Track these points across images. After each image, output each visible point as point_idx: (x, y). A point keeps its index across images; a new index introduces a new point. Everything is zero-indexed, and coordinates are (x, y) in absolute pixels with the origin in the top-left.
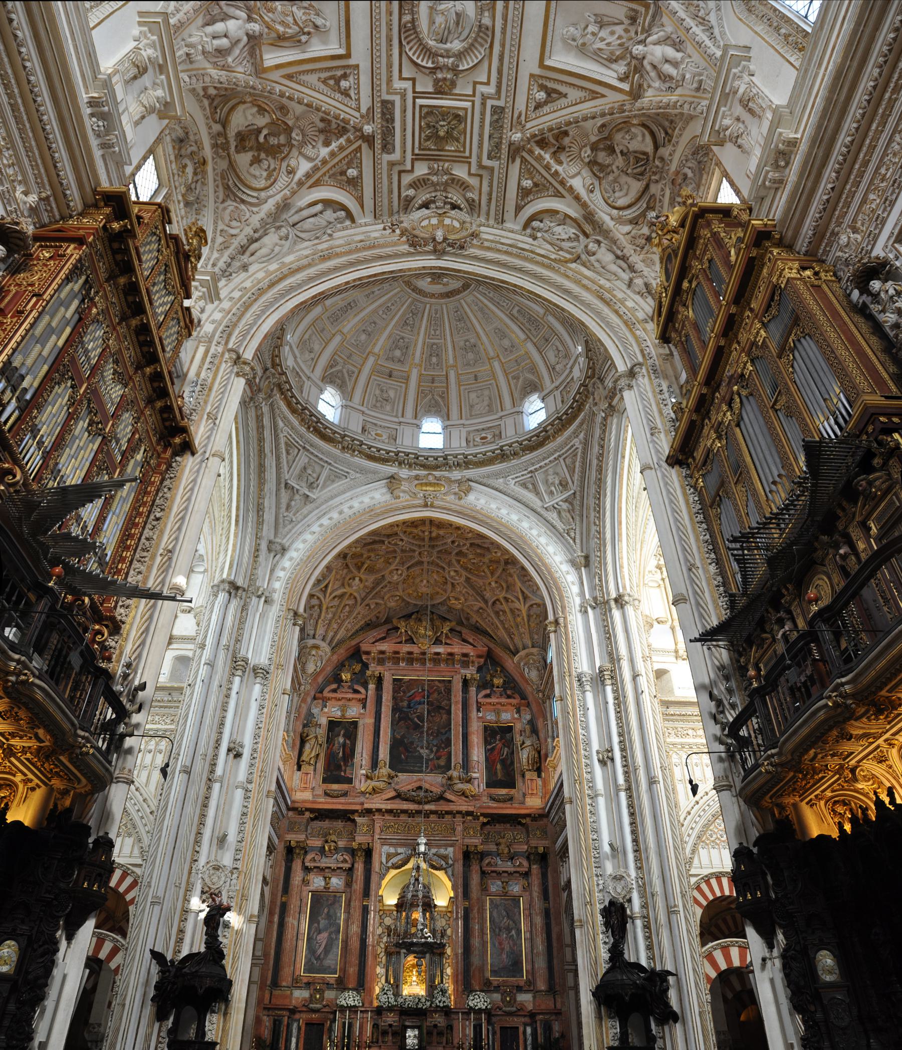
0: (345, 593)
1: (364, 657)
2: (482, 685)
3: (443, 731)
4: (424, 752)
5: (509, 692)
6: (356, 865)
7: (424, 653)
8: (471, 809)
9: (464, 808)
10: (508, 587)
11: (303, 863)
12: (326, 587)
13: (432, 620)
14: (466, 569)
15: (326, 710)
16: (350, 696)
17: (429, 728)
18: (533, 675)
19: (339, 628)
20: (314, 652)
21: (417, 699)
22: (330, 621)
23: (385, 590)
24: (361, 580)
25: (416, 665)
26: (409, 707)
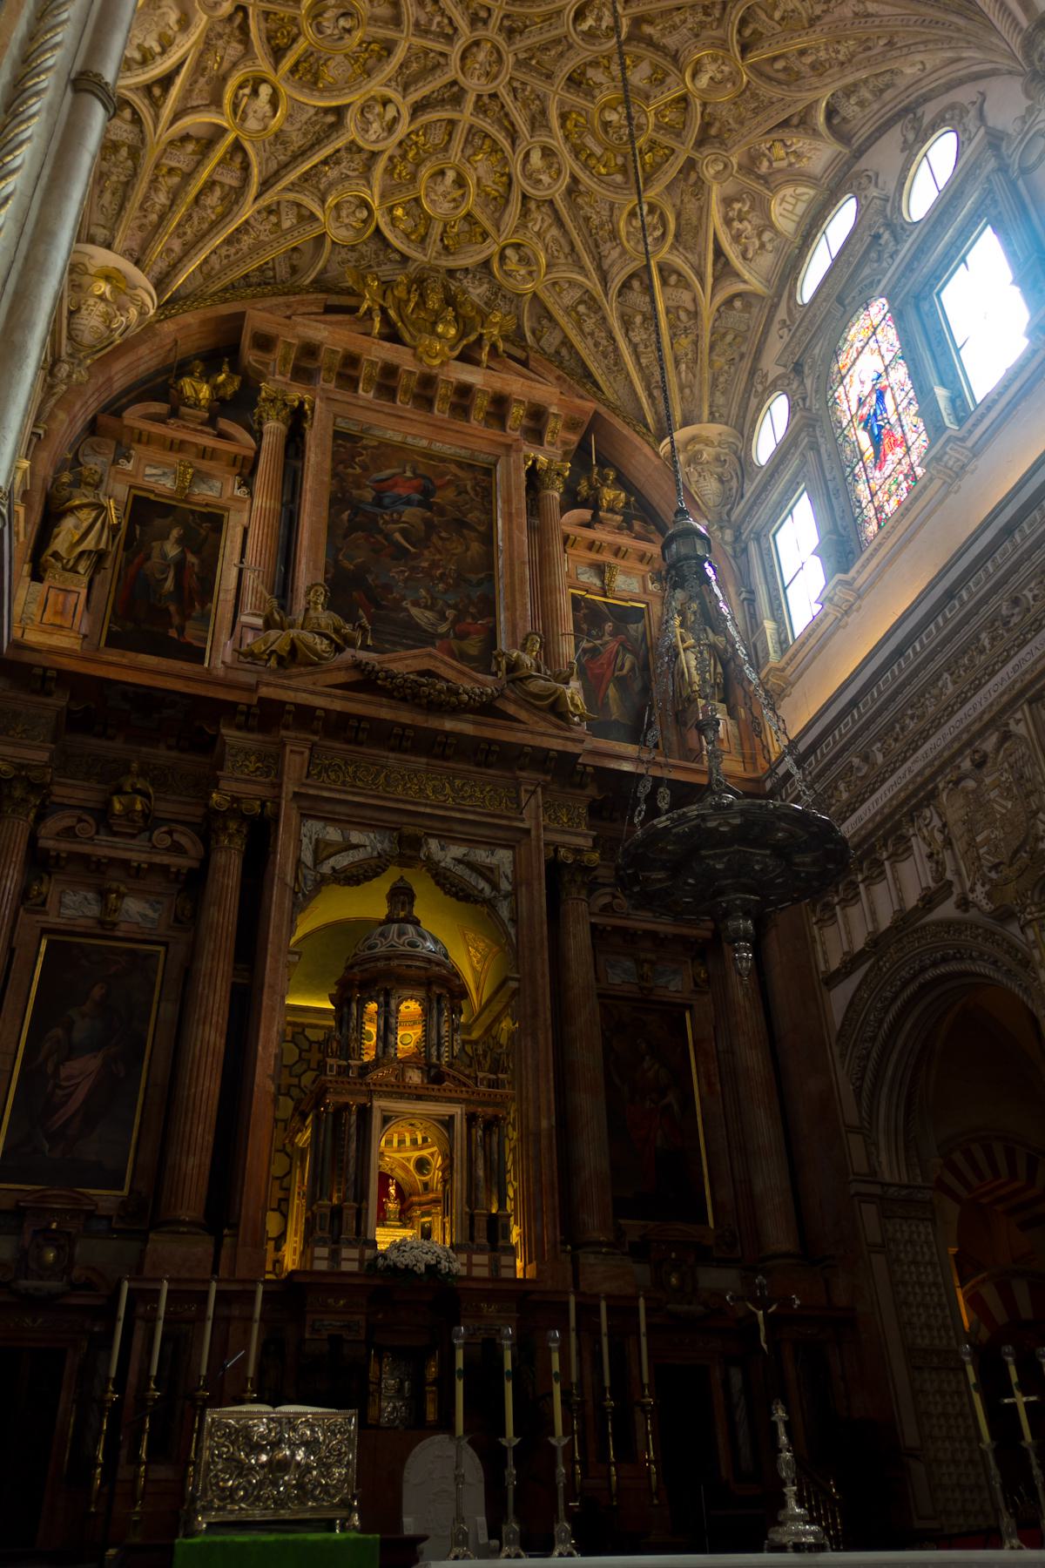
0: (220, 131)
1: (250, 356)
2: (572, 500)
3: (474, 578)
4: (422, 616)
5: (637, 525)
6: (220, 859)
7: (428, 381)
8: (572, 748)
9: (556, 744)
10: (677, 236)
11: (33, 839)
12: (166, 81)
13: (450, 300)
14: (576, 151)
15: (129, 467)
16: (208, 441)
17: (434, 565)
18: (708, 488)
19: (189, 249)
20: (103, 288)
21: (402, 491)
22: (162, 217)
23: (332, 173)
24: (274, 102)
25: (403, 404)
26: (378, 501)
